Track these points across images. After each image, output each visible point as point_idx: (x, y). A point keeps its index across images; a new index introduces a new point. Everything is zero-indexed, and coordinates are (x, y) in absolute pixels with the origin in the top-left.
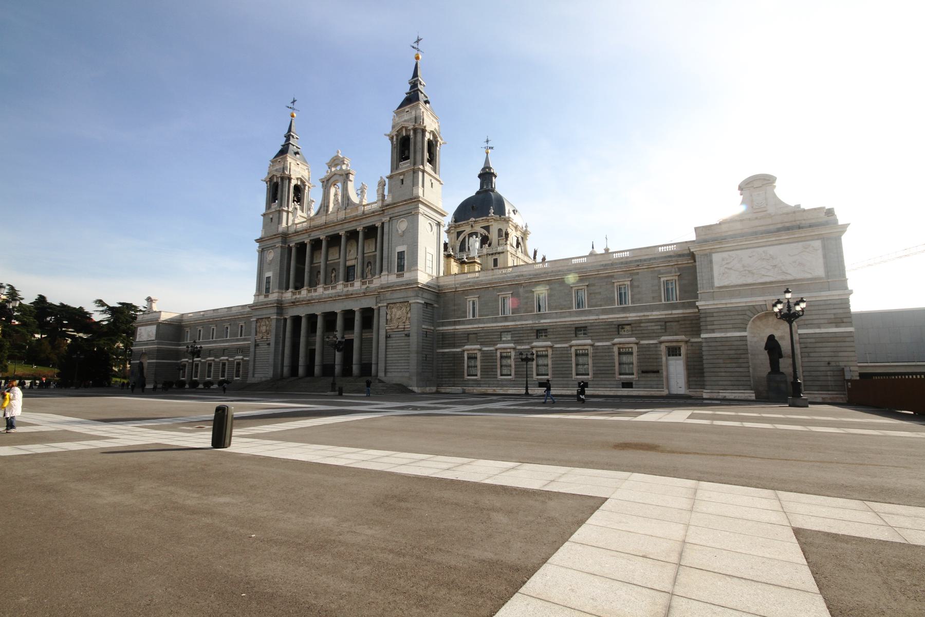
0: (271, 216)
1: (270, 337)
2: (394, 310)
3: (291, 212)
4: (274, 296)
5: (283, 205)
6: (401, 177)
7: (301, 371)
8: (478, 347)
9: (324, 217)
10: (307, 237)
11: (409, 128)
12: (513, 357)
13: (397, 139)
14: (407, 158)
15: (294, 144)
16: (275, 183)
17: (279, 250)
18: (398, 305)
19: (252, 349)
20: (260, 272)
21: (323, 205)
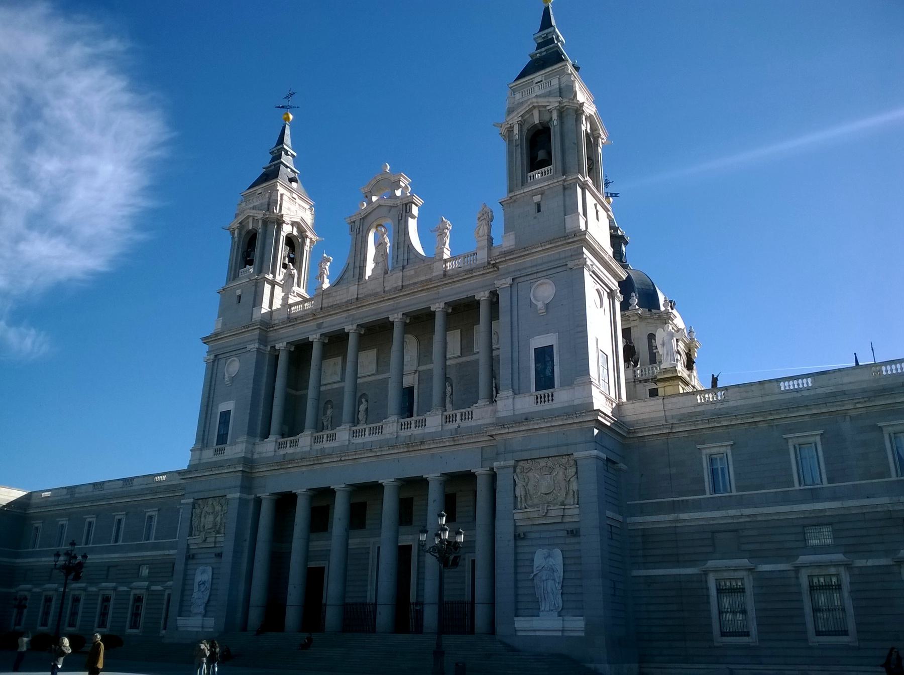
0: (238, 292)
1: (222, 539)
2: (534, 475)
3: (278, 284)
4: (236, 449)
5: (264, 270)
6: (537, 198)
7: (292, 616)
8: (745, 562)
9: (353, 289)
10: (315, 328)
11: (548, 108)
12: (846, 587)
13: (521, 130)
14: (547, 162)
15: (288, 165)
16: (249, 232)
17: (253, 358)
18: (543, 463)
19: (180, 567)
20: (208, 402)
21: (351, 266)
